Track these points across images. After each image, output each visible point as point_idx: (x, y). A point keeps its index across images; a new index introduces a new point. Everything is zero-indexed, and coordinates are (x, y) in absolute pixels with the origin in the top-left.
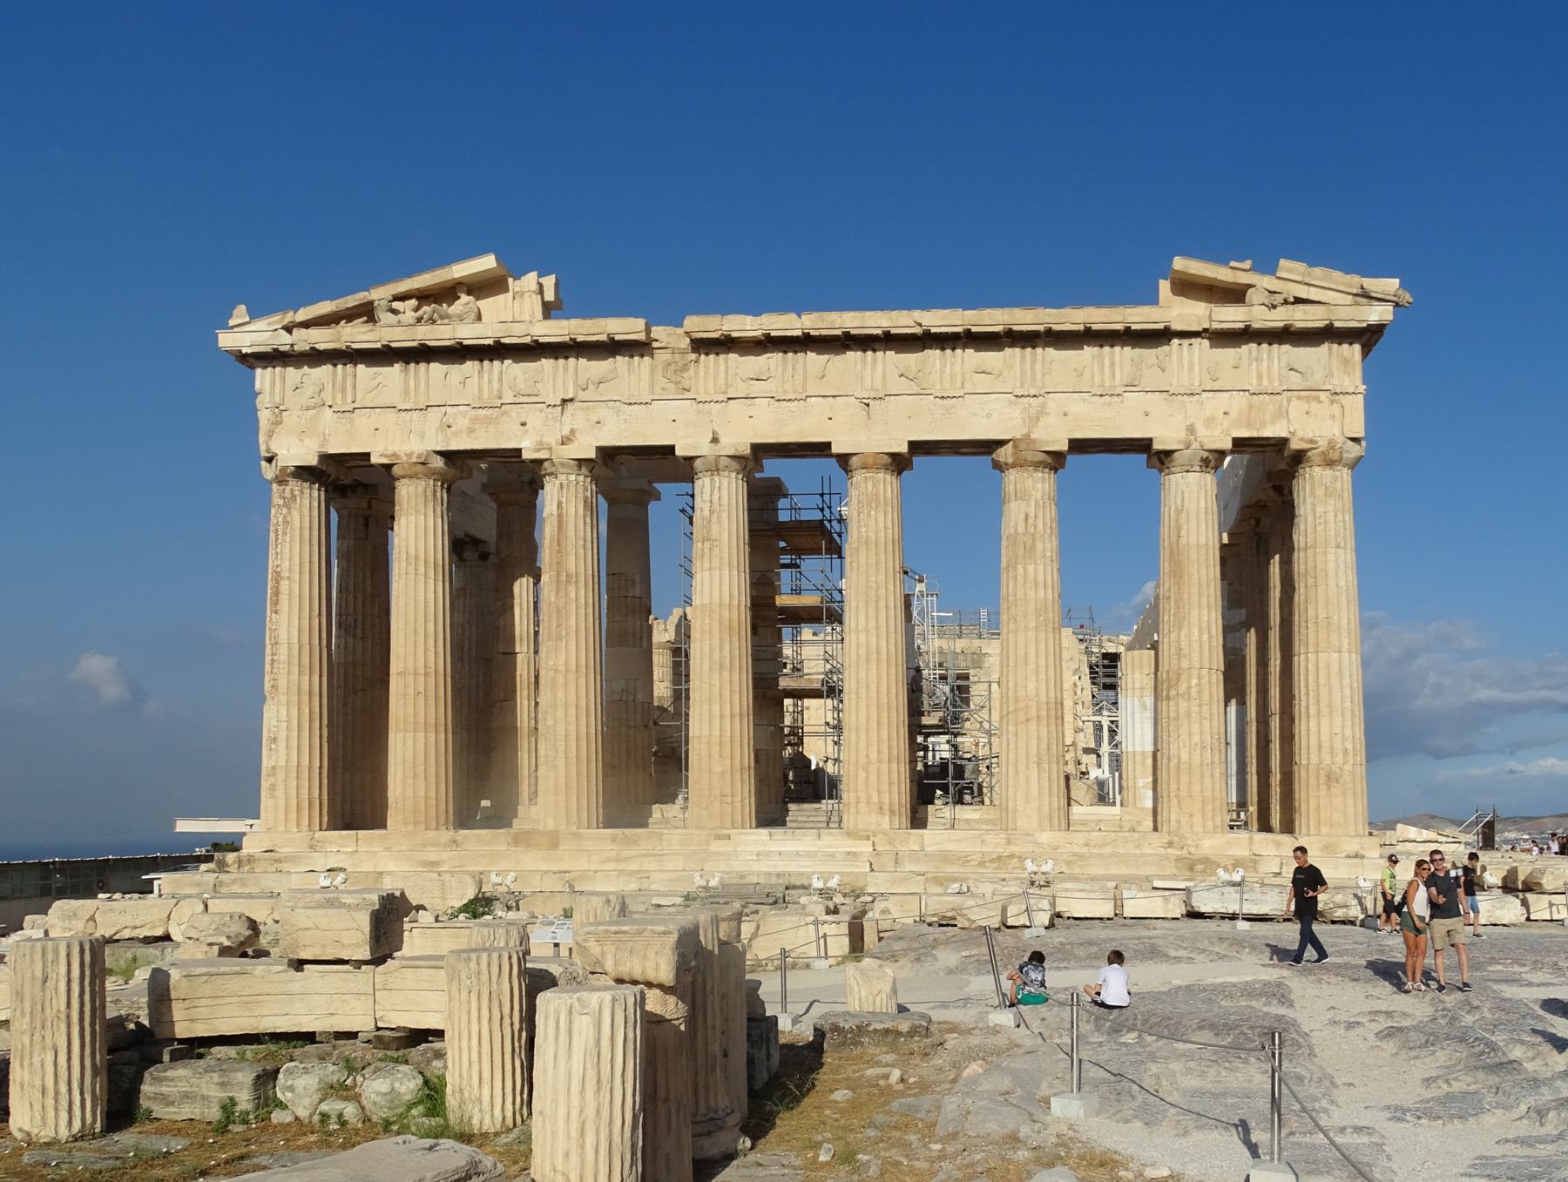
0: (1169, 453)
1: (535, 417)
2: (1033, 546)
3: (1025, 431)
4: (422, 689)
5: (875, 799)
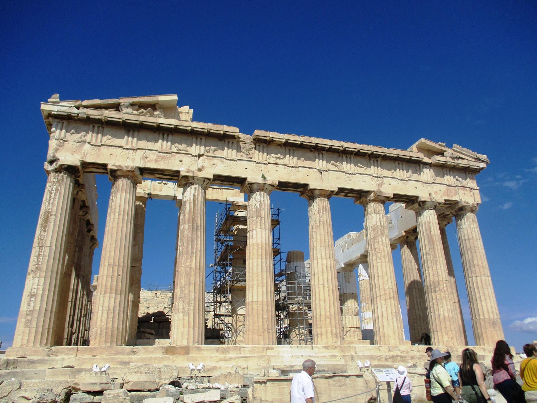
0: (424, 202)
1: (186, 159)
2: (384, 230)
3: (377, 189)
4: (121, 273)
5: (334, 331)
